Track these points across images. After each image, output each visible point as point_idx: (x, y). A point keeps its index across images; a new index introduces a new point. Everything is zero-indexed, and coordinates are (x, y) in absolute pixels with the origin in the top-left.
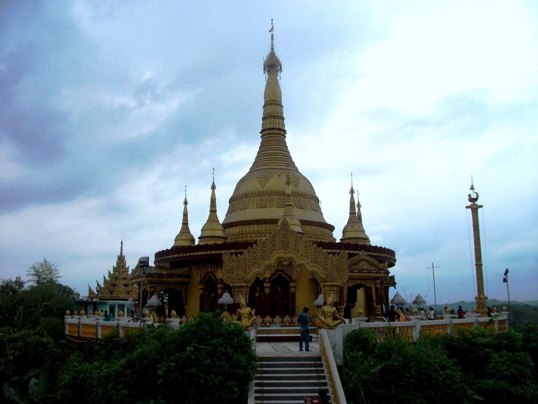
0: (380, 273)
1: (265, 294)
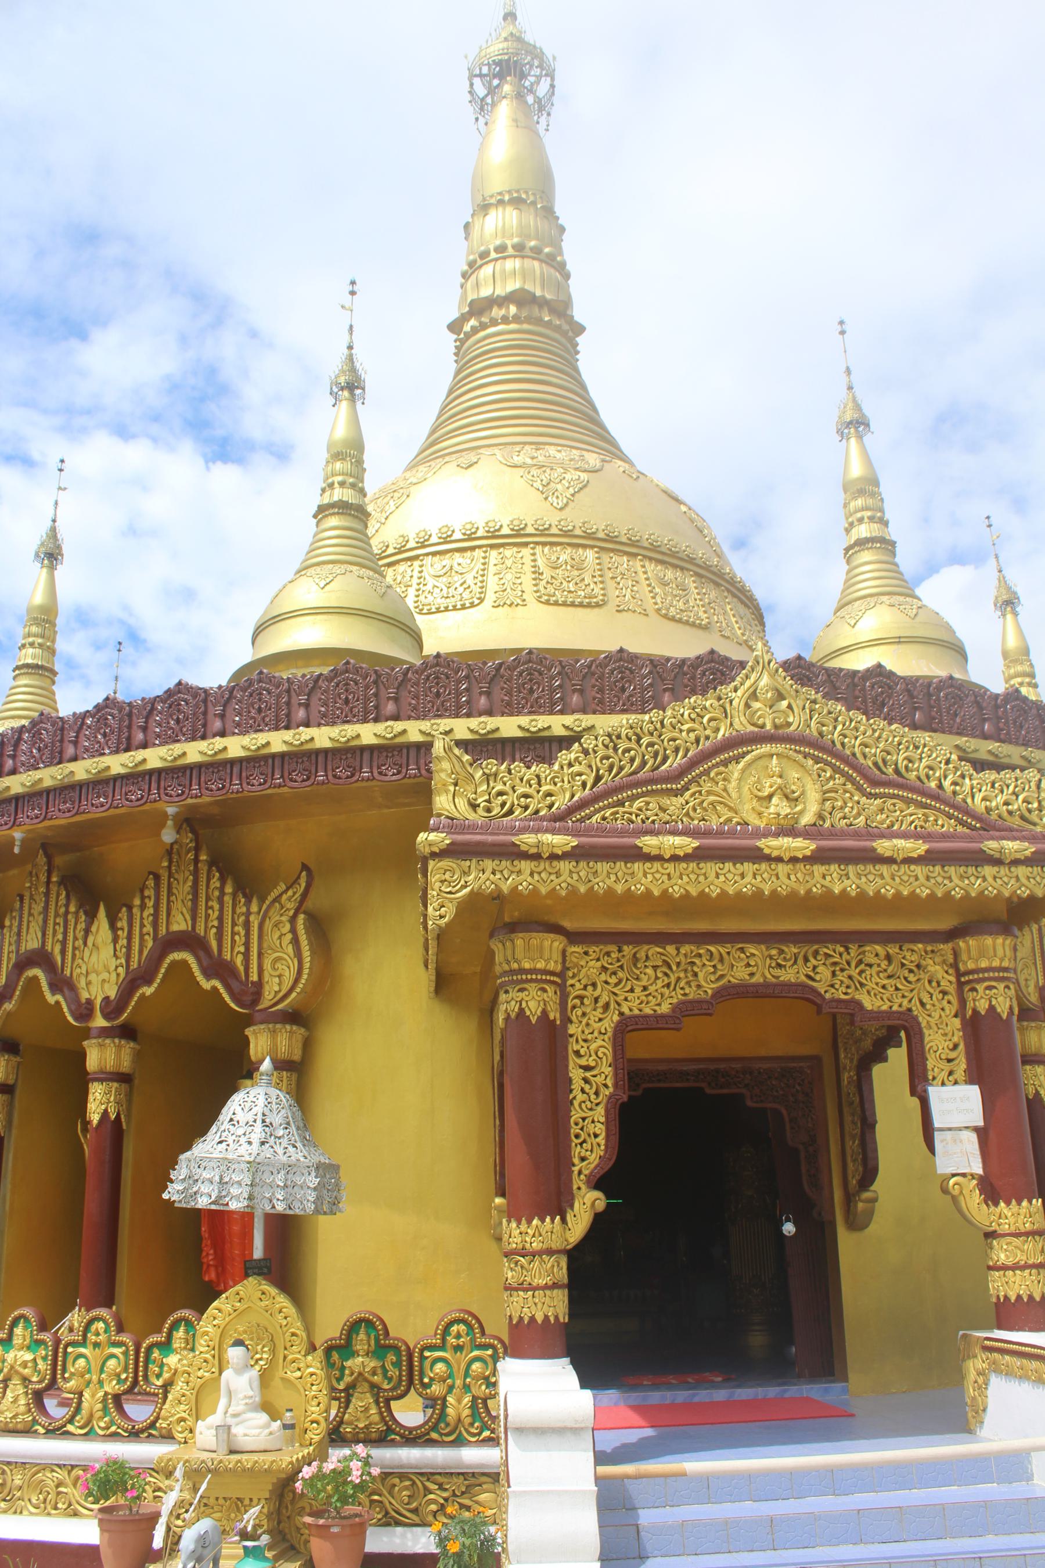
0: (980, 859)
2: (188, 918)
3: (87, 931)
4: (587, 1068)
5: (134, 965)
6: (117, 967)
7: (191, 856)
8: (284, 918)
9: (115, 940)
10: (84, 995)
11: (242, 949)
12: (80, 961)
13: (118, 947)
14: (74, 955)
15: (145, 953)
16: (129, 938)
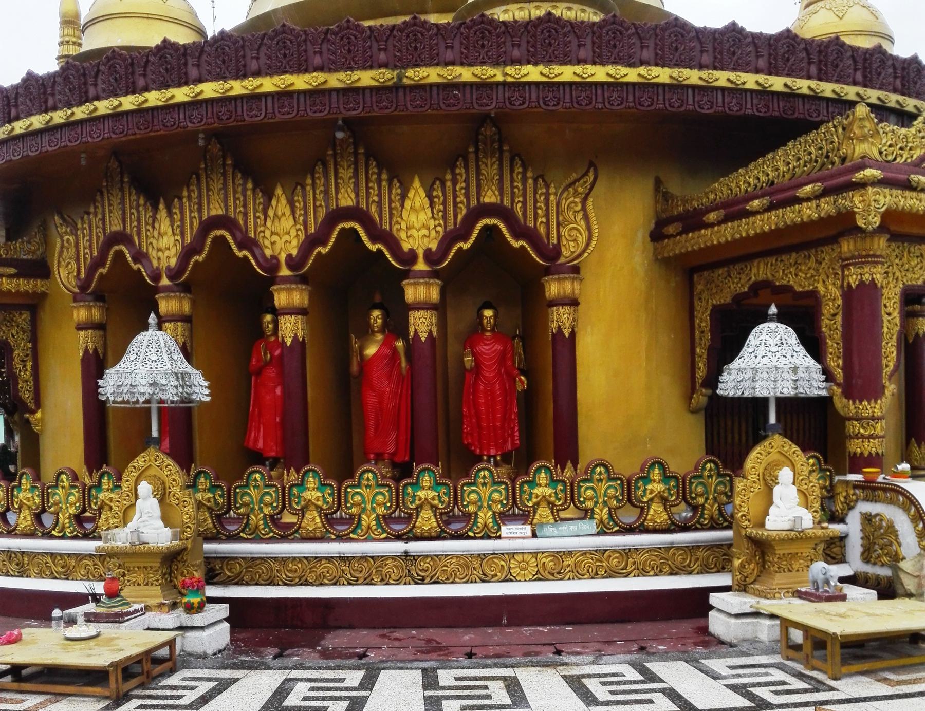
1: (412, 346)
2: (497, 193)
3: (404, 197)
4: (889, 314)
5: (451, 226)
6: (435, 226)
7: (496, 146)
8: (577, 200)
9: (432, 205)
10: (406, 246)
11: (544, 220)
12: (399, 219)
13: (435, 211)
14: (391, 215)
15: (460, 217)
16: (444, 203)
